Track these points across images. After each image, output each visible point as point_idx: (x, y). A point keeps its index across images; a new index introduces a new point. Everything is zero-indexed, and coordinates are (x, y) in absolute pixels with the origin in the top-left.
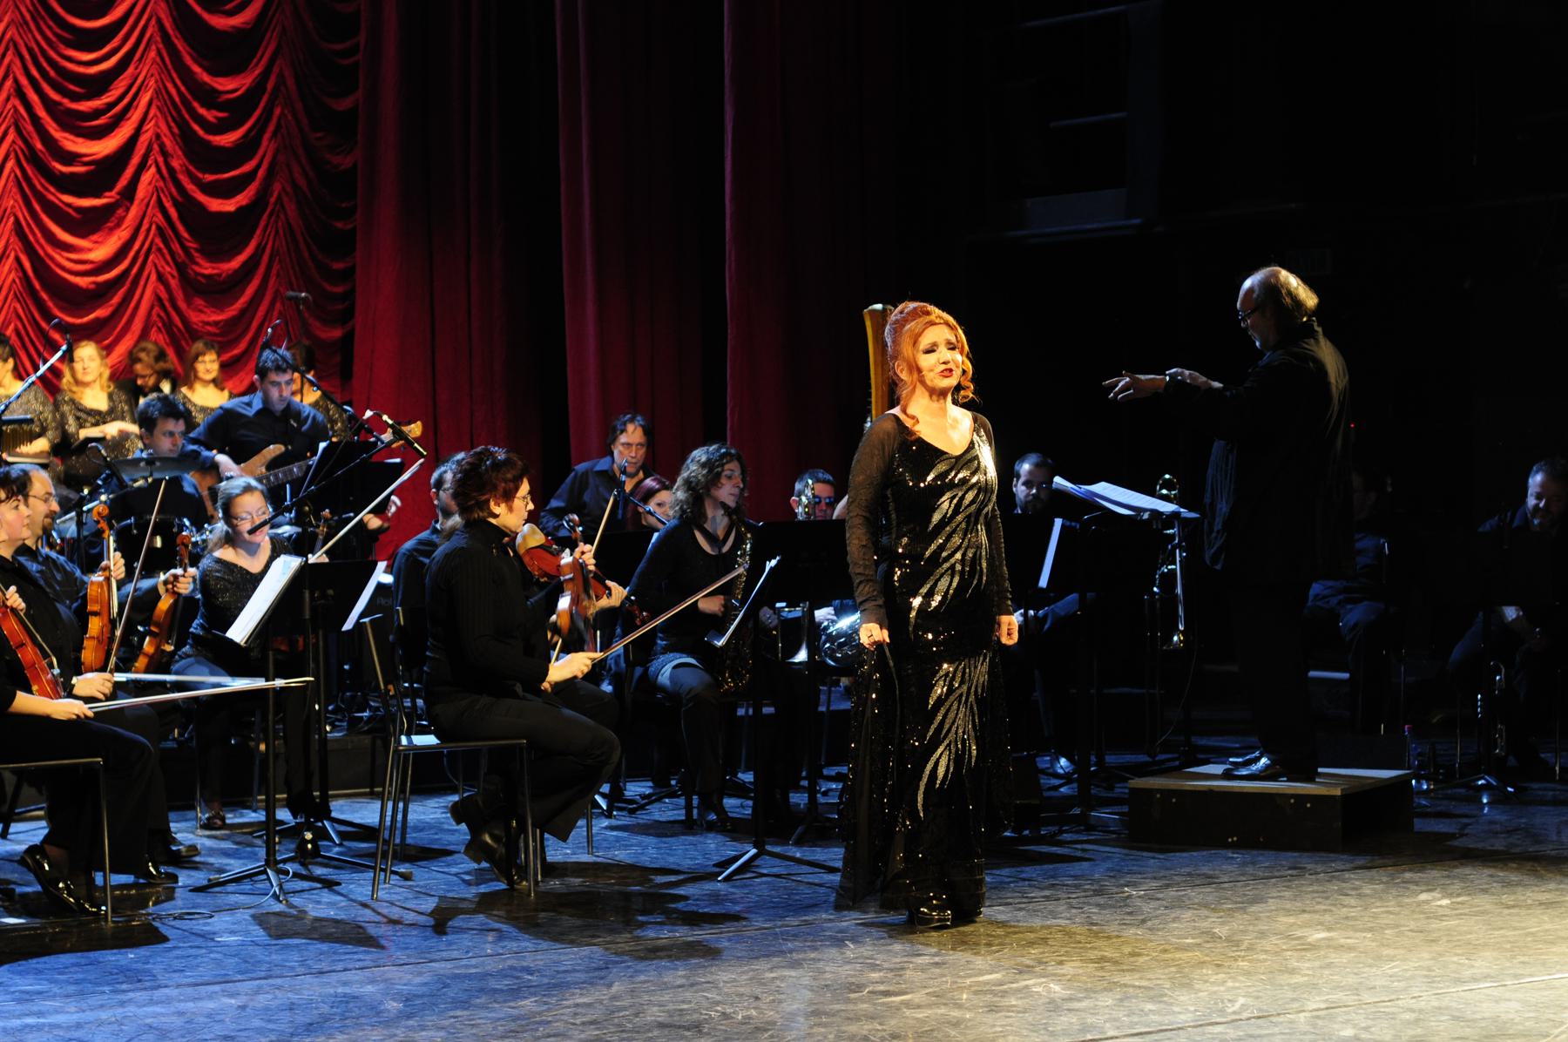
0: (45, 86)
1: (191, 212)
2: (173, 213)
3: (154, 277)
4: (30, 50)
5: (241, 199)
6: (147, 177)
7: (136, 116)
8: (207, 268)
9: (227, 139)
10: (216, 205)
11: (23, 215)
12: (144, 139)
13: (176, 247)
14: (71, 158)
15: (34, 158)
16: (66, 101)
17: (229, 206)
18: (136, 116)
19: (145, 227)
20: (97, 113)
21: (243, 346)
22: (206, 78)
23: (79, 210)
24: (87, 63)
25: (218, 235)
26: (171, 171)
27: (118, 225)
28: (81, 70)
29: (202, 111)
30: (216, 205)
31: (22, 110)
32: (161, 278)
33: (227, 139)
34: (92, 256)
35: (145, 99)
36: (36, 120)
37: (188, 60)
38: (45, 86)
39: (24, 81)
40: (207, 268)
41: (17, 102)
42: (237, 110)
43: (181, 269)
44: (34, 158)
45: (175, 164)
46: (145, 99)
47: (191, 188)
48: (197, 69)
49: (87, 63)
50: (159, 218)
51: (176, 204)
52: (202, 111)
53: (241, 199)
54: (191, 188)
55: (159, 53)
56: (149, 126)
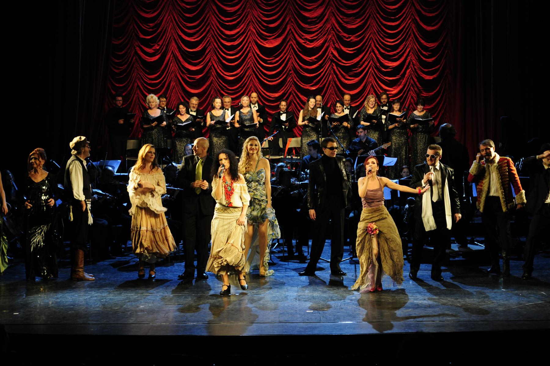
0: (379, 48)
1: (420, 79)
2: (415, 80)
3: (410, 98)
4: (376, 40)
5: (435, 76)
6: (408, 71)
7: (405, 55)
8: (425, 94)
9: (430, 60)
10: (428, 77)
11: (374, 82)
12: (408, 61)
13: (416, 89)
14: (387, 67)
15: (377, 68)
16: (386, 53)
17: (431, 78)
18: (405, 55)
19: (408, 84)
20: (395, 55)
21: (436, 115)
22: (425, 44)
23: (389, 80)
24: (391, 42)
25: (427, 85)
26: (415, 69)
27: (399, 85)
28: (390, 44)
29: (424, 53)
30: (428, 77)
31: (374, 56)
32: (412, 97)
33: (430, 60)
34: (392, 93)
35: (408, 50)
36: (377, 58)
37: (420, 39)
38: (379, 48)
39: (374, 48)
40: (425, 94)
41: (372, 54)
42: (434, 52)
43: (418, 95)
44: (377, 68)
45: (415, 67)
46: (408, 50)
47: (420, 73)
48: (422, 41)
49: (391, 42)
50: (412, 81)
51: (416, 77)
52: (424, 53)
53: (435, 76)
54: (420, 73)
55: (412, 38)
56: (409, 58)
